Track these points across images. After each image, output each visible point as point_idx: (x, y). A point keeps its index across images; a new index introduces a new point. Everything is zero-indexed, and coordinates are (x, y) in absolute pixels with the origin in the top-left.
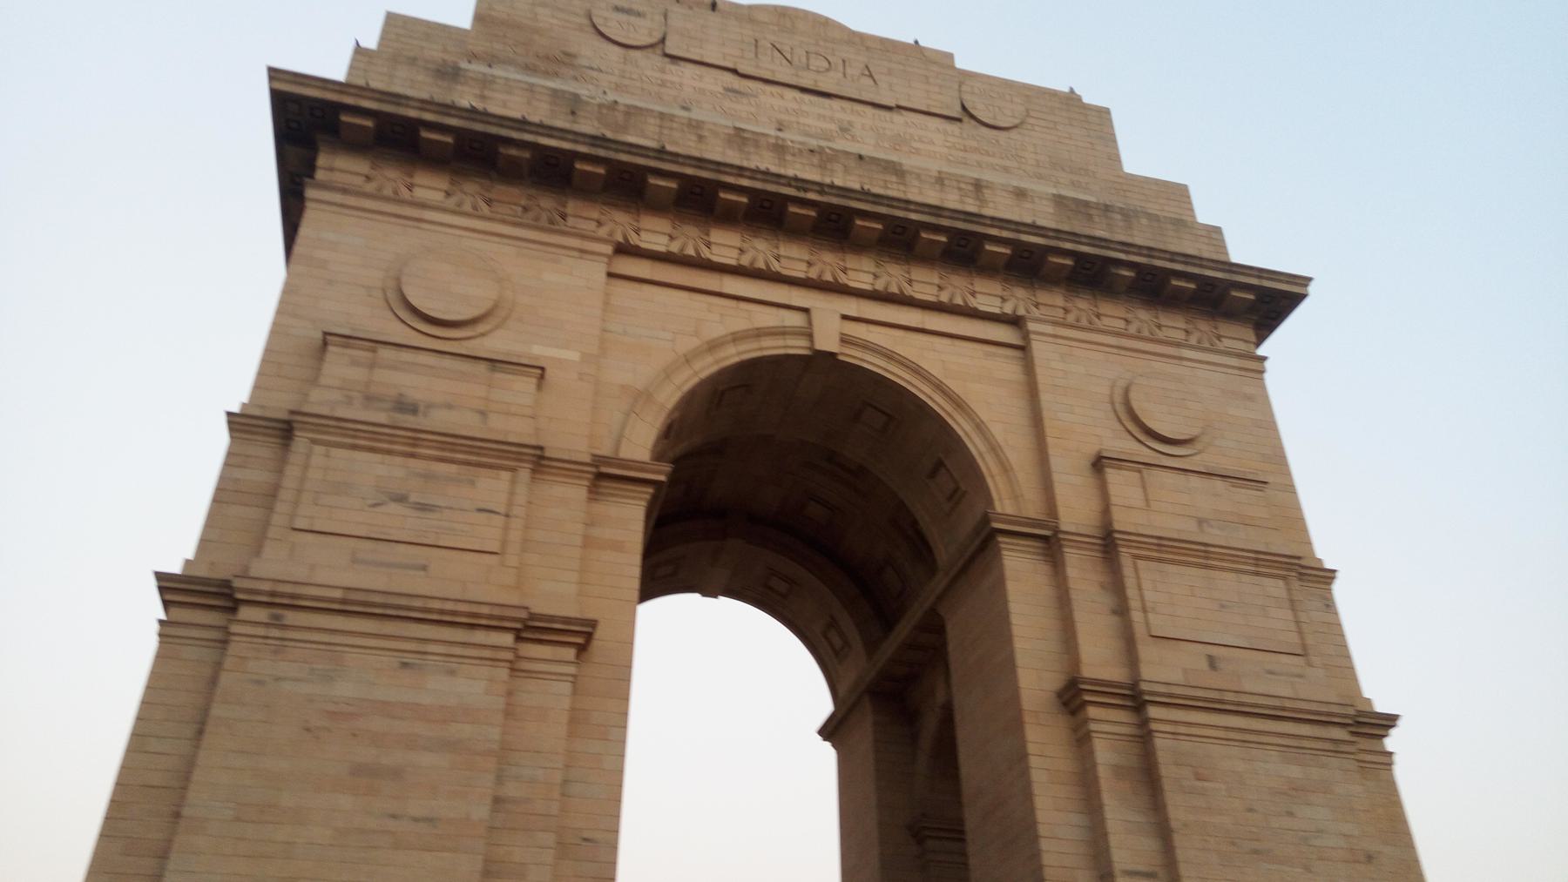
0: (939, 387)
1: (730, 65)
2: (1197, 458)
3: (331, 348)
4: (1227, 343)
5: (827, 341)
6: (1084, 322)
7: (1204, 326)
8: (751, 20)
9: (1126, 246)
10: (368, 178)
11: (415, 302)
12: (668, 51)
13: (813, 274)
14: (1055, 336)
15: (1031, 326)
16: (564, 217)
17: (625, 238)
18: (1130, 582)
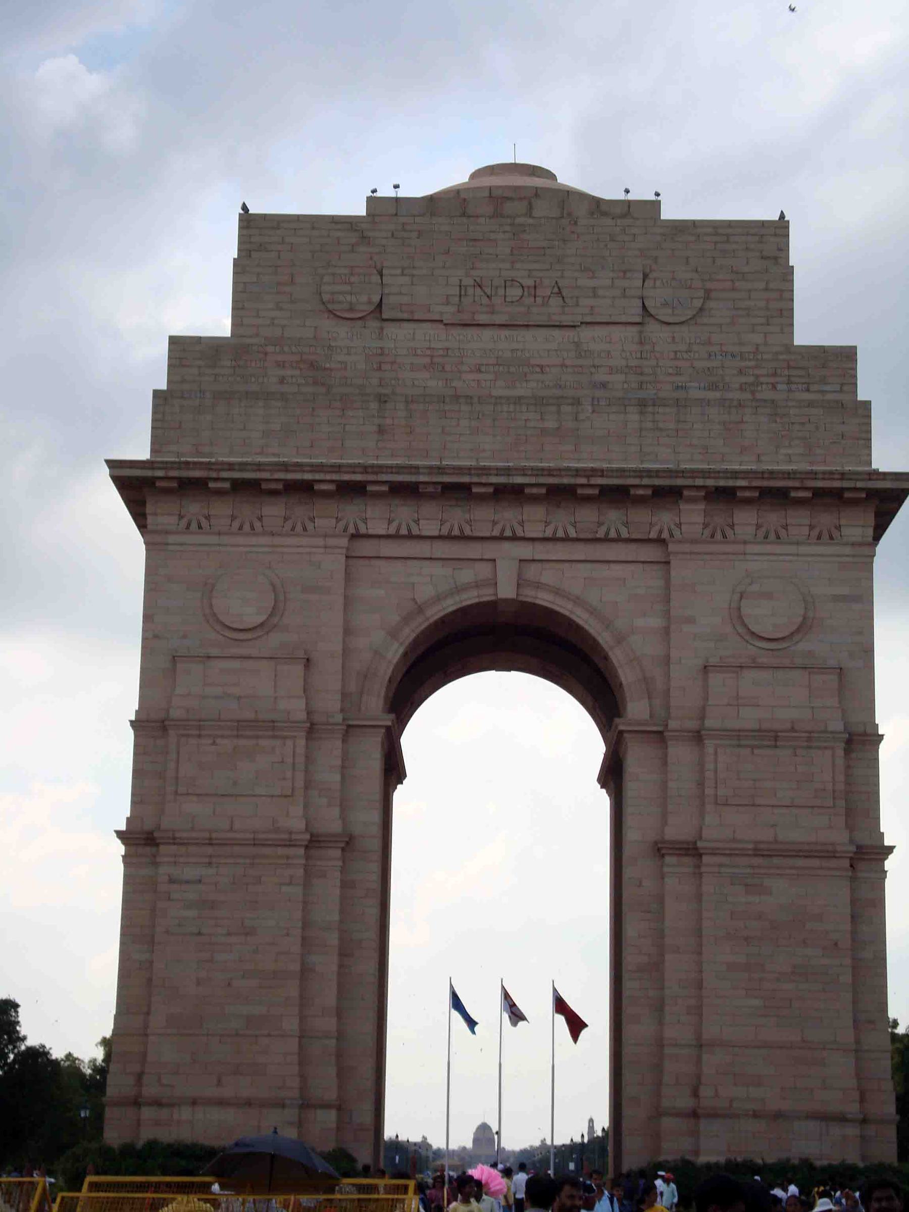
0: (592, 611)
1: (437, 317)
2: (792, 648)
3: (178, 665)
4: (845, 531)
5: (506, 591)
6: (719, 536)
7: (826, 519)
8: (464, 214)
9: (746, 474)
10: (181, 517)
11: (222, 618)
12: (384, 316)
13: (496, 533)
14: (691, 553)
15: (672, 547)
16: (312, 520)
17: (357, 529)
18: (710, 766)
